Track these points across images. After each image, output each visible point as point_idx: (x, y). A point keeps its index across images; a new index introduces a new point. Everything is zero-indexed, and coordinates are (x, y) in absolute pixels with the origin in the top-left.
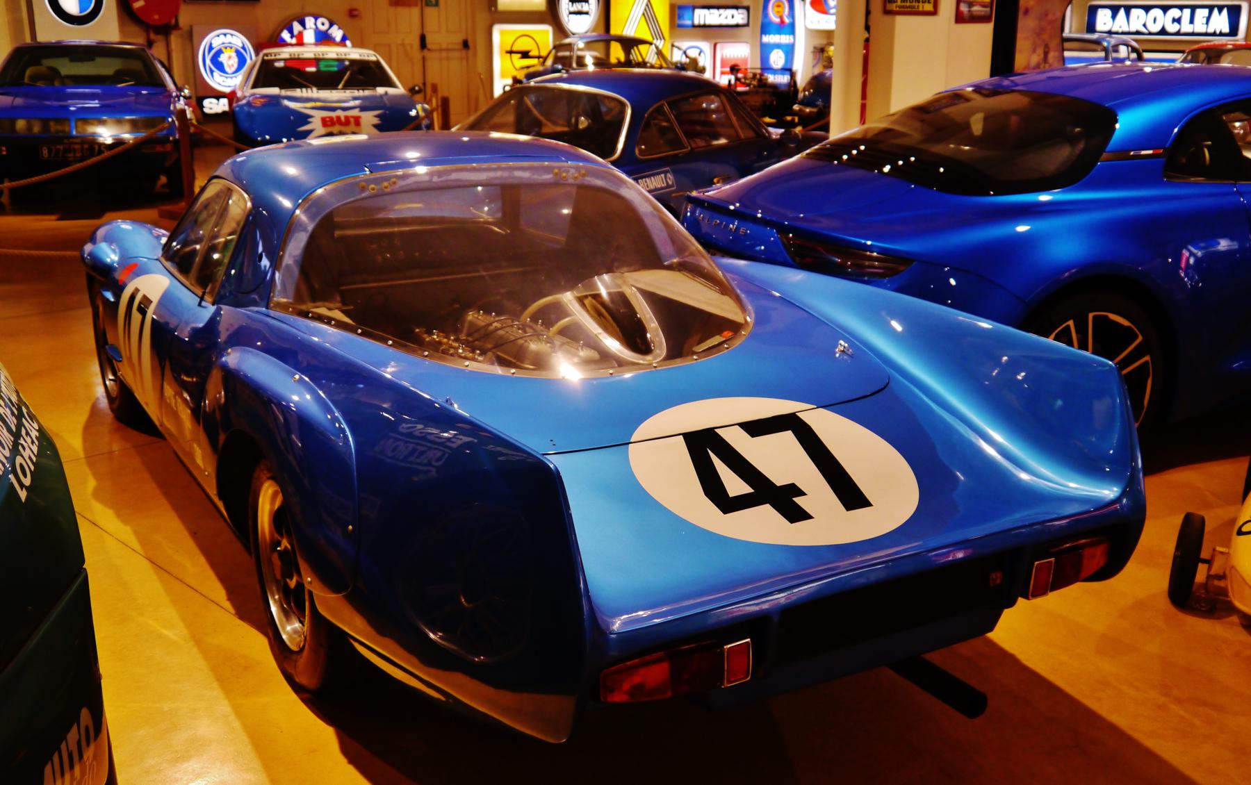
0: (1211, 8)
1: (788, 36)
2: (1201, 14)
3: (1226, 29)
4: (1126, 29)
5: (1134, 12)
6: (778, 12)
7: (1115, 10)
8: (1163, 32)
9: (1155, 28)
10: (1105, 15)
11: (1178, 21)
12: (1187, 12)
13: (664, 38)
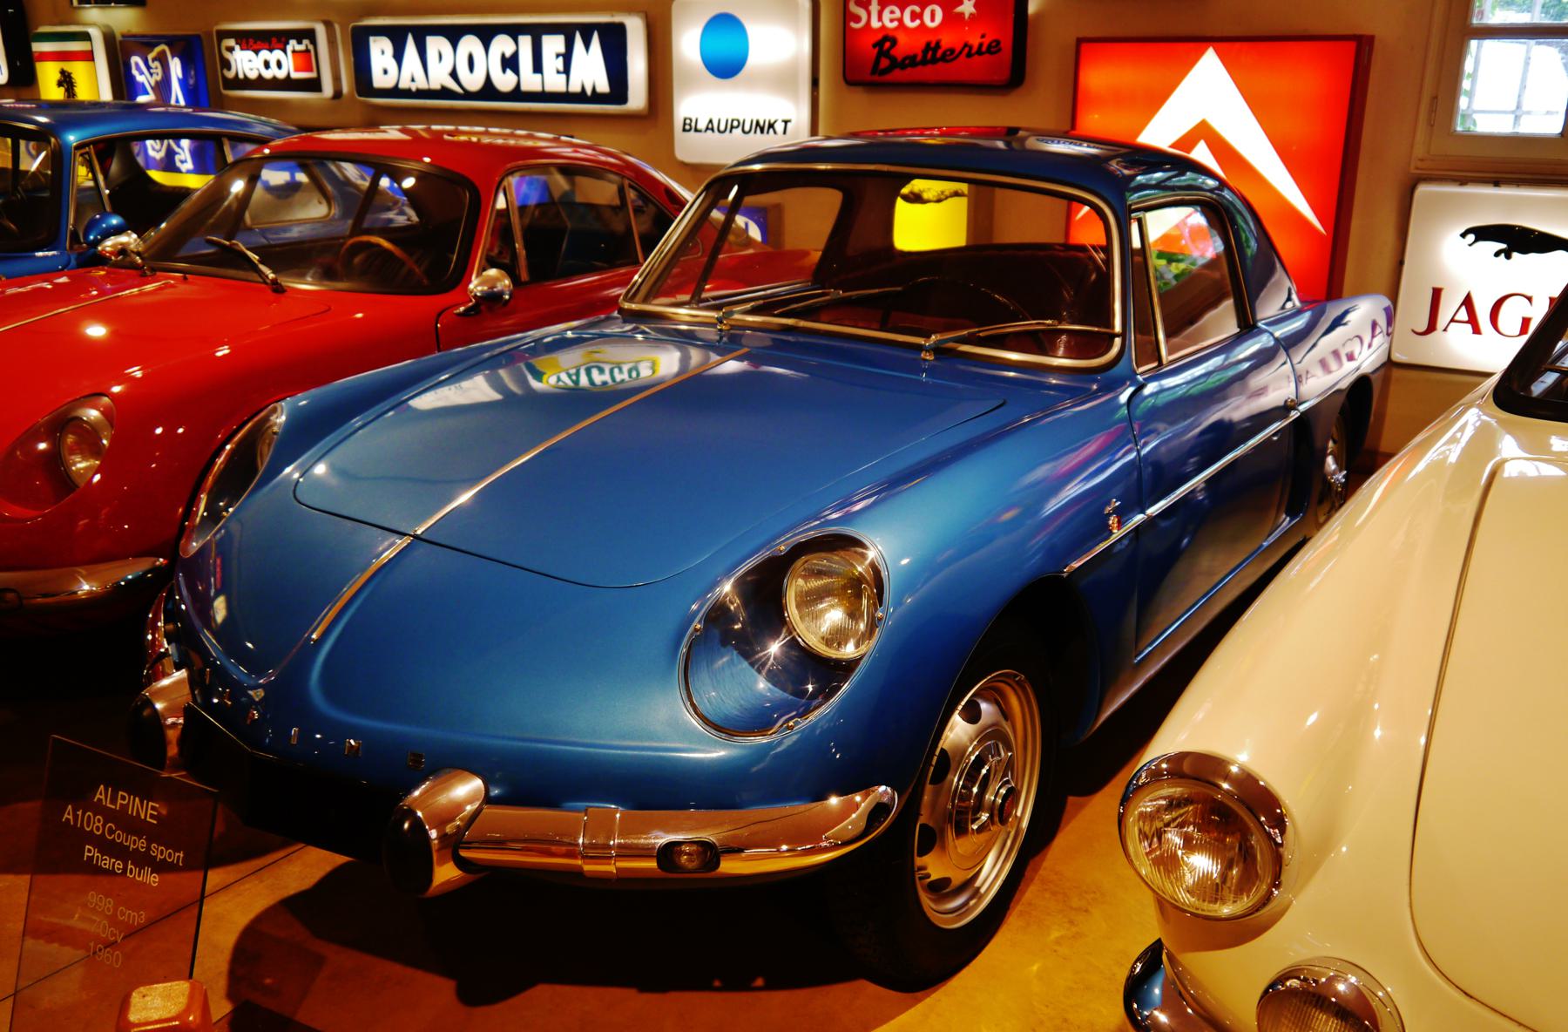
0: (567, 31)
2: (553, 45)
3: (603, 86)
4: (421, 83)
5: (435, 44)
7: (397, 37)
8: (489, 90)
9: (473, 82)
10: (383, 53)
11: (510, 63)
12: (526, 42)
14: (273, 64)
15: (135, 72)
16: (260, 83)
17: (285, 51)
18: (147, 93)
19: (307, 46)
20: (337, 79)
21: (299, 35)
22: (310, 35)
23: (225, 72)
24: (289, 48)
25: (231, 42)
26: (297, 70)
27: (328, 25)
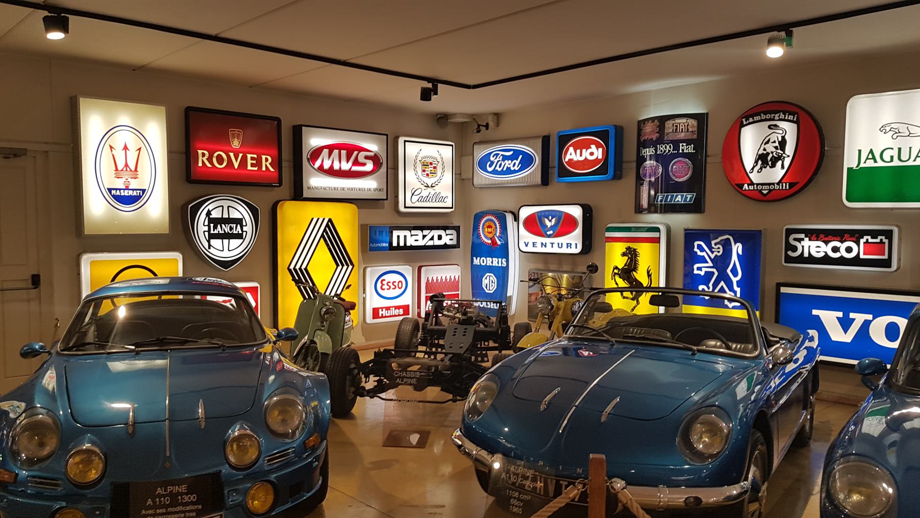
1: (500, 260)
6: (490, 233)
13: (352, 264)
14: (843, 250)
15: (696, 249)
16: (826, 260)
17: (858, 244)
18: (707, 262)
19: (881, 240)
20: (899, 260)
21: (874, 234)
22: (889, 234)
23: (790, 253)
24: (862, 241)
25: (802, 236)
26: (865, 254)
27: (898, 226)
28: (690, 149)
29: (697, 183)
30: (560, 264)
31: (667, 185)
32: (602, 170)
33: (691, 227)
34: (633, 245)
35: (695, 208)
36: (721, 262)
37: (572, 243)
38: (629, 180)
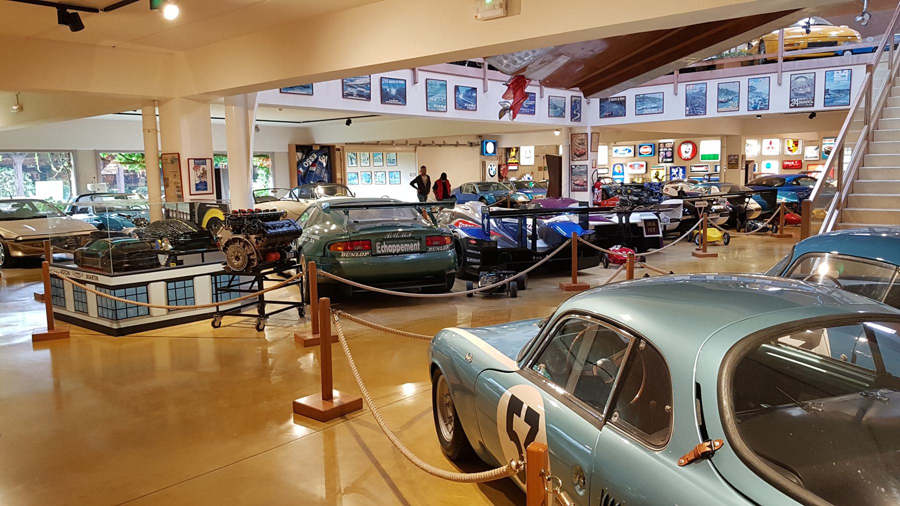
22: (708, 166)
28: (671, 150)
29: (672, 157)
30: (639, 176)
31: (666, 157)
32: (651, 154)
33: (671, 166)
34: (658, 170)
35: (672, 162)
36: (678, 173)
37: (643, 170)
38: (657, 156)
